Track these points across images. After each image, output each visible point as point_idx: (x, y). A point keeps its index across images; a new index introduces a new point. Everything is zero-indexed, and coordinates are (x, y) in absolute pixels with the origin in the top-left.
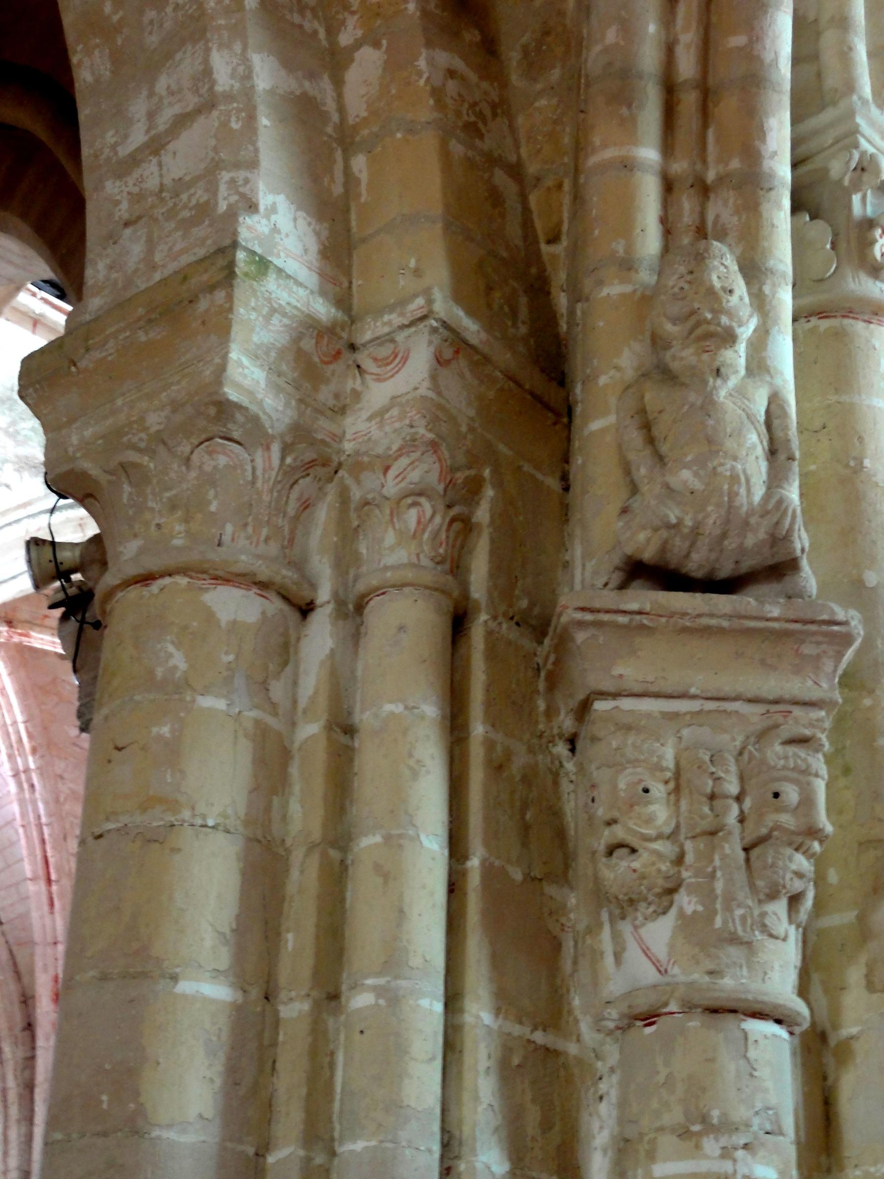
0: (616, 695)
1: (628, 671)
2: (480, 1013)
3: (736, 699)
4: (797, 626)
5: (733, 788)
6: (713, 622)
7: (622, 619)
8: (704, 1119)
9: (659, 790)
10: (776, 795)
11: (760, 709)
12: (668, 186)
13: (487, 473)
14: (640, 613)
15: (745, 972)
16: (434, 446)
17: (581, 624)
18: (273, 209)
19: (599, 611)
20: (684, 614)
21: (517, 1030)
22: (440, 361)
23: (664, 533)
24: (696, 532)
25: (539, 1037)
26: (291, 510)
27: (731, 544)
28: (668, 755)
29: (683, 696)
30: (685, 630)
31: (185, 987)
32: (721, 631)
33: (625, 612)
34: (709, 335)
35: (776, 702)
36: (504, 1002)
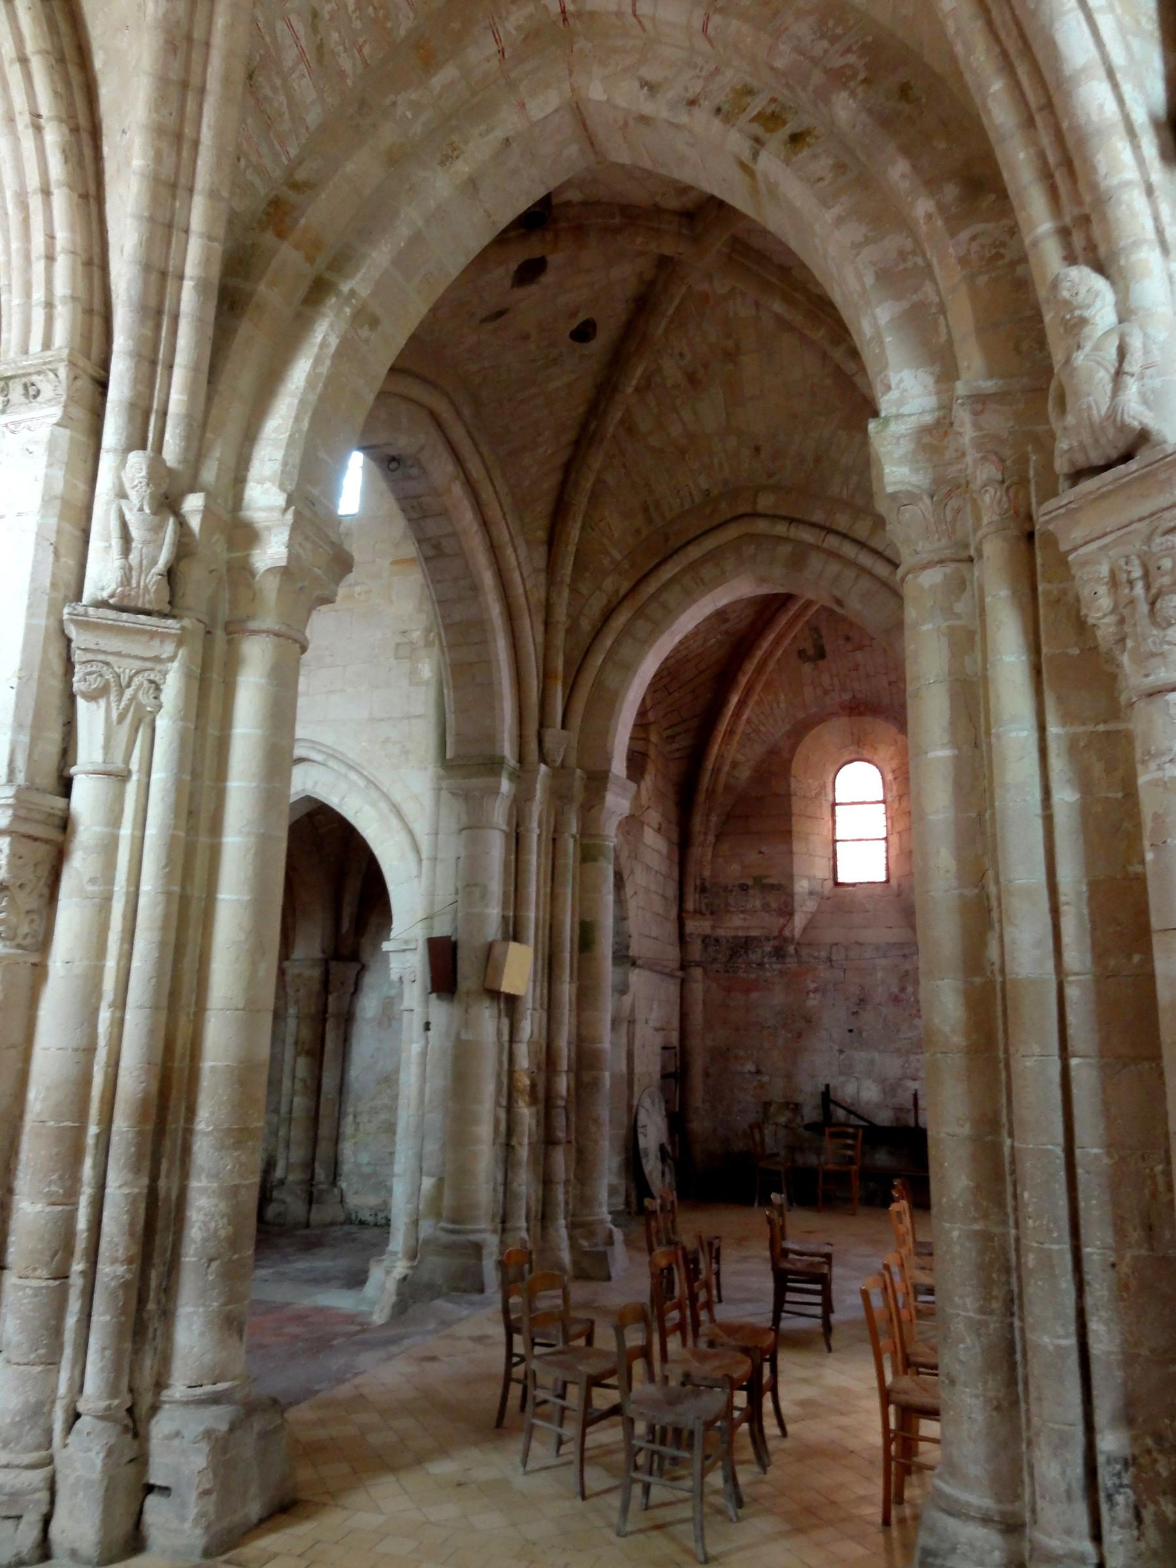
0: (1075, 549)
1: (1077, 534)
2: (1053, 730)
3: (1131, 523)
4: (1146, 470)
5: (1137, 573)
6: (1104, 489)
7: (1063, 510)
8: (1149, 753)
9: (1102, 590)
10: (1159, 568)
11: (1147, 522)
12: (1064, 233)
13: (1030, 448)
14: (1070, 503)
15: (1163, 669)
16: (984, 458)
17: (1048, 522)
18: (901, 381)
19: (1051, 512)
20: (1091, 493)
21: (1081, 729)
22: (975, 413)
23: (1067, 456)
24: (1082, 446)
25: (1101, 728)
26: (949, 515)
27: (1103, 441)
28: (1104, 570)
29: (1105, 535)
30: (1094, 500)
31: (931, 755)
32: (1110, 492)
33: (1061, 507)
34: (1075, 325)
35: (1152, 514)
36: (1067, 718)
